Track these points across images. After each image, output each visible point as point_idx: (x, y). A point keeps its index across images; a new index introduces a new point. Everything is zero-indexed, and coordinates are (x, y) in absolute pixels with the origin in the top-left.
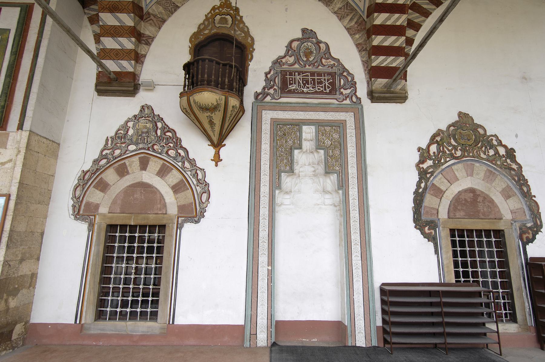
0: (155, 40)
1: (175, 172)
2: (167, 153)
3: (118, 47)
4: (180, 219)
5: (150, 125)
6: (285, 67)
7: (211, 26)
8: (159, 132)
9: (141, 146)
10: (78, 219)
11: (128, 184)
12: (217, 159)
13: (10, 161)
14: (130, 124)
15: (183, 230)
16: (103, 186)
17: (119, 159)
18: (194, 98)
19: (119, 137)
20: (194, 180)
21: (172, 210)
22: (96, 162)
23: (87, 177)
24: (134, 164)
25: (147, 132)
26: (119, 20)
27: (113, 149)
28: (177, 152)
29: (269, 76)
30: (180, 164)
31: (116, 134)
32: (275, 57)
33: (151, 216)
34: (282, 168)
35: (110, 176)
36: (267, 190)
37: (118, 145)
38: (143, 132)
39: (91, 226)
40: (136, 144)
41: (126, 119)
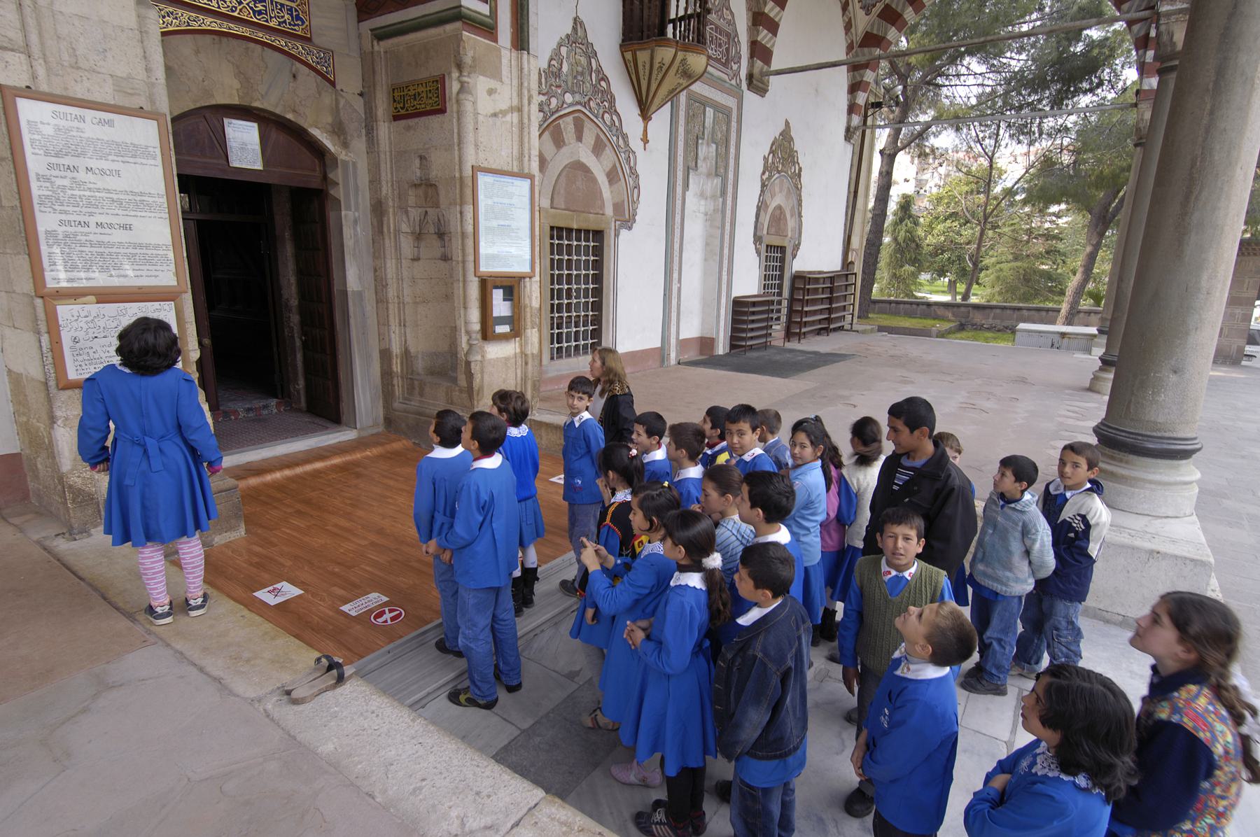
4: (618, 223)
9: (578, 97)
12: (645, 140)
15: (621, 237)
17: (557, 115)
18: (687, 57)
19: (552, 72)
20: (627, 167)
28: (612, 119)
30: (615, 138)
31: (549, 66)
37: (553, 88)
40: (573, 93)
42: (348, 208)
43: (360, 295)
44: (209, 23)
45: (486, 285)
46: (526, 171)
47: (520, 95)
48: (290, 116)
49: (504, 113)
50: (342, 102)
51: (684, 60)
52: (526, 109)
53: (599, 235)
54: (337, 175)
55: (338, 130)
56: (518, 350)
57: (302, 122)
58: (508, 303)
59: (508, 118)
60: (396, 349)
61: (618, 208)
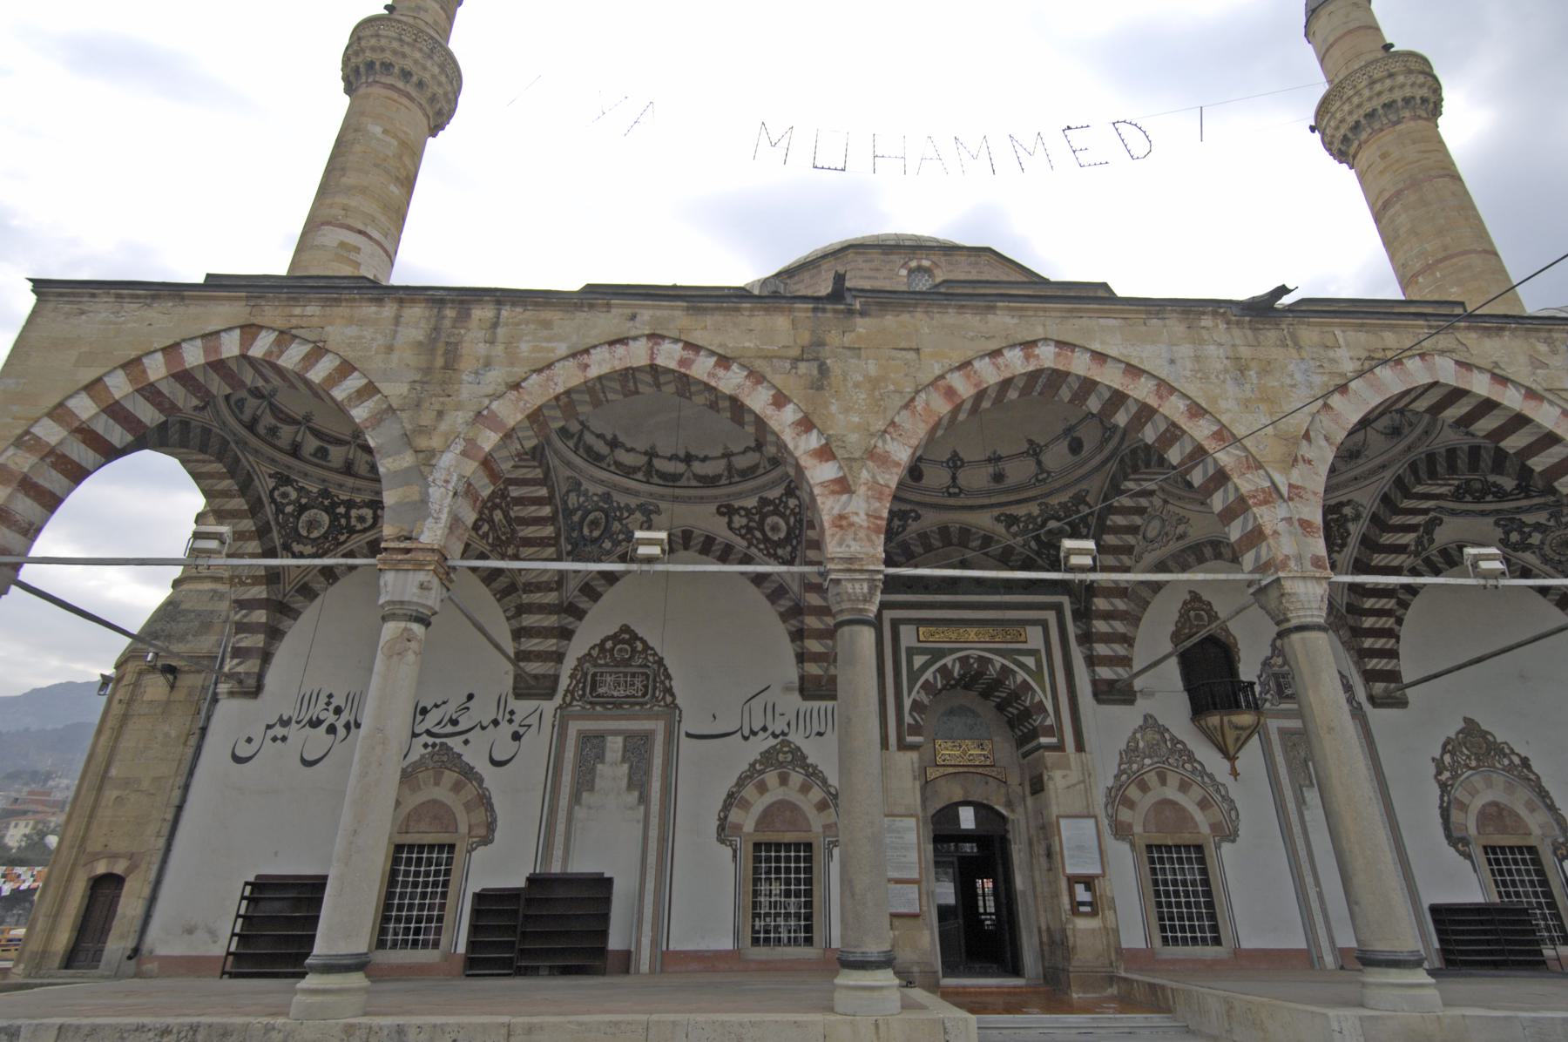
0: (1137, 640)
1: (1195, 787)
2: (1183, 766)
3: (1111, 653)
4: (1217, 839)
5: (1157, 737)
6: (1276, 669)
7: (1188, 625)
8: (1168, 743)
9: (1156, 759)
10: (1117, 839)
11: (1153, 801)
12: (1234, 773)
13: (1079, 782)
14: (1138, 736)
16: (1131, 805)
21: (1205, 829)
22: (1117, 777)
23: (1113, 794)
24: (1152, 779)
25: (1157, 744)
26: (1111, 626)
27: (1130, 763)
29: (1262, 679)
30: (1199, 779)
31: (1128, 746)
32: (1262, 659)
33: (1187, 836)
34: (1302, 783)
35: (1133, 792)
36: (1294, 807)
38: (1153, 745)
39: (1133, 846)
40: (1150, 757)
41: (1132, 730)
42: (1015, 843)
43: (1024, 893)
44: (951, 770)
45: (1073, 880)
46: (1092, 813)
47: (1083, 774)
48: (985, 802)
49: (1074, 785)
50: (1010, 790)
51: (1230, 721)
52: (1087, 781)
53: (1199, 848)
54: (1009, 827)
55: (1009, 804)
56: (1102, 925)
57: (991, 804)
58: (1089, 894)
59: (1078, 787)
60: (1044, 927)
61: (1215, 827)
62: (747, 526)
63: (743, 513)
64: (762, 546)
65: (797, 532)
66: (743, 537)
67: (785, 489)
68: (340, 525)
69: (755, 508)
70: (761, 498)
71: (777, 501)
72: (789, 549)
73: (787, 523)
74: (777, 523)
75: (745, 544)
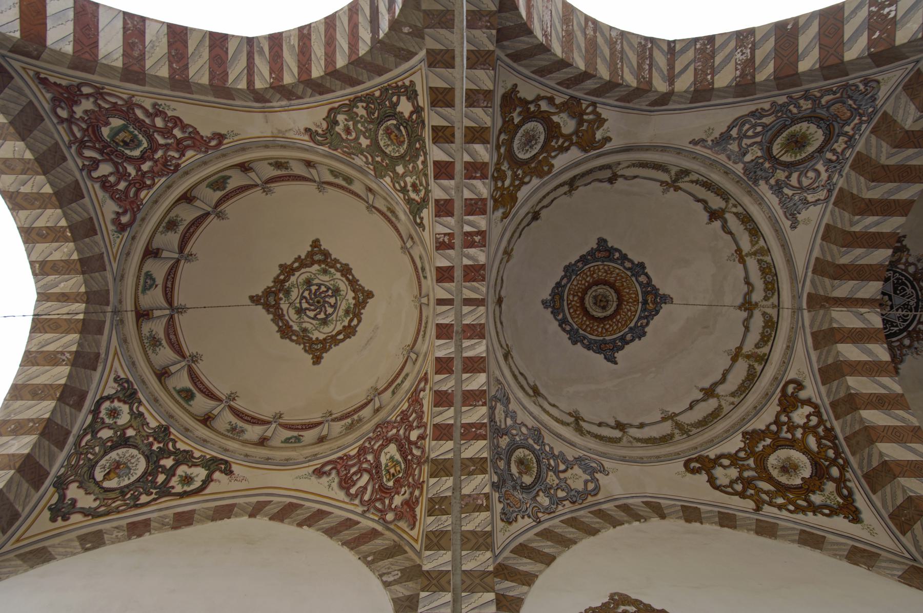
62: (740, 478)
63: (726, 462)
64: (780, 501)
65: (831, 453)
66: (742, 495)
67: (780, 403)
68: (154, 481)
69: (740, 450)
70: (745, 434)
71: (774, 428)
72: (830, 487)
73: (806, 451)
74: (789, 459)
75: (750, 504)
